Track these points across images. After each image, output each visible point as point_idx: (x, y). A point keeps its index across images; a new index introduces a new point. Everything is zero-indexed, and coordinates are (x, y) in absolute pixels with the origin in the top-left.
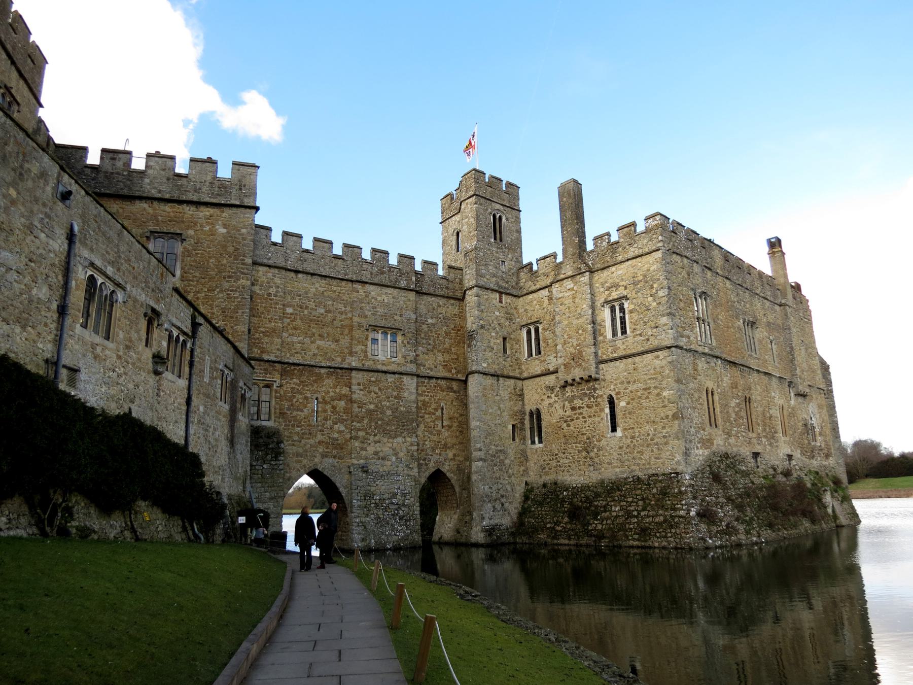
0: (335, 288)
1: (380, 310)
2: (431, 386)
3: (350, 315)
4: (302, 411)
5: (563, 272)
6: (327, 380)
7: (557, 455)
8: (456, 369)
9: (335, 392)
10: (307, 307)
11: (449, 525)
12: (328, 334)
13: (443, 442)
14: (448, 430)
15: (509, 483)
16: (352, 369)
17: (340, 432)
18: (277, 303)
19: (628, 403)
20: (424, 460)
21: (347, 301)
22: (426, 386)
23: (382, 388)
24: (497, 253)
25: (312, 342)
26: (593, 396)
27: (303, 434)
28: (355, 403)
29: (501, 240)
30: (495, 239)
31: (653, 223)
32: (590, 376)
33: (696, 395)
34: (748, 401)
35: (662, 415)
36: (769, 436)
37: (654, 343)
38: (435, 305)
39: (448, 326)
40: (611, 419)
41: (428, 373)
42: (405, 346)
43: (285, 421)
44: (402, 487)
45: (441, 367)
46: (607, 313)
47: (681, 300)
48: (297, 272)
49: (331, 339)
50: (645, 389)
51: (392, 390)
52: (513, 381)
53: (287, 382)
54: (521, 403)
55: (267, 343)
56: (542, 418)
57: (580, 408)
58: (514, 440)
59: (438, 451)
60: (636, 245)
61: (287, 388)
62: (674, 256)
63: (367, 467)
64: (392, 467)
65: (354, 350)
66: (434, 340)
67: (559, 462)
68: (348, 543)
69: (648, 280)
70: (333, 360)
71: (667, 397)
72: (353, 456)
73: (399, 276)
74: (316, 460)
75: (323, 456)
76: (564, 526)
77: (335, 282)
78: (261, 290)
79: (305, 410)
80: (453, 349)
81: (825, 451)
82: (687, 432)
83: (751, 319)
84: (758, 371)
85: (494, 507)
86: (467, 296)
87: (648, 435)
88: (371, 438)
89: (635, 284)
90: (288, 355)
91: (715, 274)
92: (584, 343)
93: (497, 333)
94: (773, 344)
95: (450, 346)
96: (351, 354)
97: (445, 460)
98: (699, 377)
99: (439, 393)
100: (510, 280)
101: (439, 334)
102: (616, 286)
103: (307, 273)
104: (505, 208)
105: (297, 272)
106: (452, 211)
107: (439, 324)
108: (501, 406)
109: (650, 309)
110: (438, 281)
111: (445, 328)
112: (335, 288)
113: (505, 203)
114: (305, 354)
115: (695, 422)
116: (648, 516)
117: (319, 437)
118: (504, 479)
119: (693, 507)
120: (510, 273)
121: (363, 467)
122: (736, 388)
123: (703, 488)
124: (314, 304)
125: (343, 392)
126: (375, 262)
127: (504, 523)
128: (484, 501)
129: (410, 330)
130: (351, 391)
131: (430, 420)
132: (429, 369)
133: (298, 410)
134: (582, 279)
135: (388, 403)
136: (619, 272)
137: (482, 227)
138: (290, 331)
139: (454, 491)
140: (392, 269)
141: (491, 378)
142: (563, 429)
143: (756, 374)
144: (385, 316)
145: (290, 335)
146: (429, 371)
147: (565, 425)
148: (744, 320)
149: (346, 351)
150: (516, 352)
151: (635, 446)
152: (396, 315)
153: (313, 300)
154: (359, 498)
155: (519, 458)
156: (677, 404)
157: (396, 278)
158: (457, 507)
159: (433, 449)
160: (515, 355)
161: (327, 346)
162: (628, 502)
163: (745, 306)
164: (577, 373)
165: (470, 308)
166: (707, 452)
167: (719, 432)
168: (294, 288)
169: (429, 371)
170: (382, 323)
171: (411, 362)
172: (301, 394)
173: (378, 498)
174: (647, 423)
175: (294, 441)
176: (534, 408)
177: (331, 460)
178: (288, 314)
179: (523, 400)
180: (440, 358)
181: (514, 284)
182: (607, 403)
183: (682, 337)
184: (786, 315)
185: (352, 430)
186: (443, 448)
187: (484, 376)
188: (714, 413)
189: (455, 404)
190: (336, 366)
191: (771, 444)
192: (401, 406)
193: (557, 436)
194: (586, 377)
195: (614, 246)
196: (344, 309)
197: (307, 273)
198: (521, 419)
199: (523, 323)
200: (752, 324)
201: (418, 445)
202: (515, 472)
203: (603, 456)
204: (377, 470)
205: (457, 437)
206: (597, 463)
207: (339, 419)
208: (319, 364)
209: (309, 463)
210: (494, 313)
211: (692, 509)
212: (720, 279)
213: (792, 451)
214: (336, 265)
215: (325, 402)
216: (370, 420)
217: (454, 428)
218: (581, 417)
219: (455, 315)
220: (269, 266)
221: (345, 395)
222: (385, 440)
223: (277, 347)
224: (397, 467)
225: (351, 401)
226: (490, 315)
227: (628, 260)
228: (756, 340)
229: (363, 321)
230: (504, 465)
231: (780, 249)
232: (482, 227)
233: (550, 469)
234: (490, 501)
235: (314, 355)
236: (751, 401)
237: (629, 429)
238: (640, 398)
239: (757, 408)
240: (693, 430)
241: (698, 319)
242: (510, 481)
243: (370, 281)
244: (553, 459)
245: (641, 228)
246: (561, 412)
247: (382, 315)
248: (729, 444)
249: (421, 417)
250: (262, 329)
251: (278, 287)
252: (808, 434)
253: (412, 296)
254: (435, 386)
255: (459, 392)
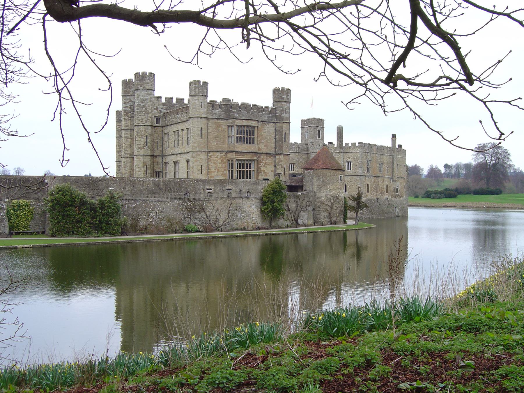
34: (378, 185)
46: (347, 164)
69: (357, 159)
102: (350, 158)
136: (351, 154)
143: (381, 178)
166: (366, 199)
191: (382, 195)
195: (350, 147)
239: (380, 187)
245: (357, 145)
253: (297, 154)
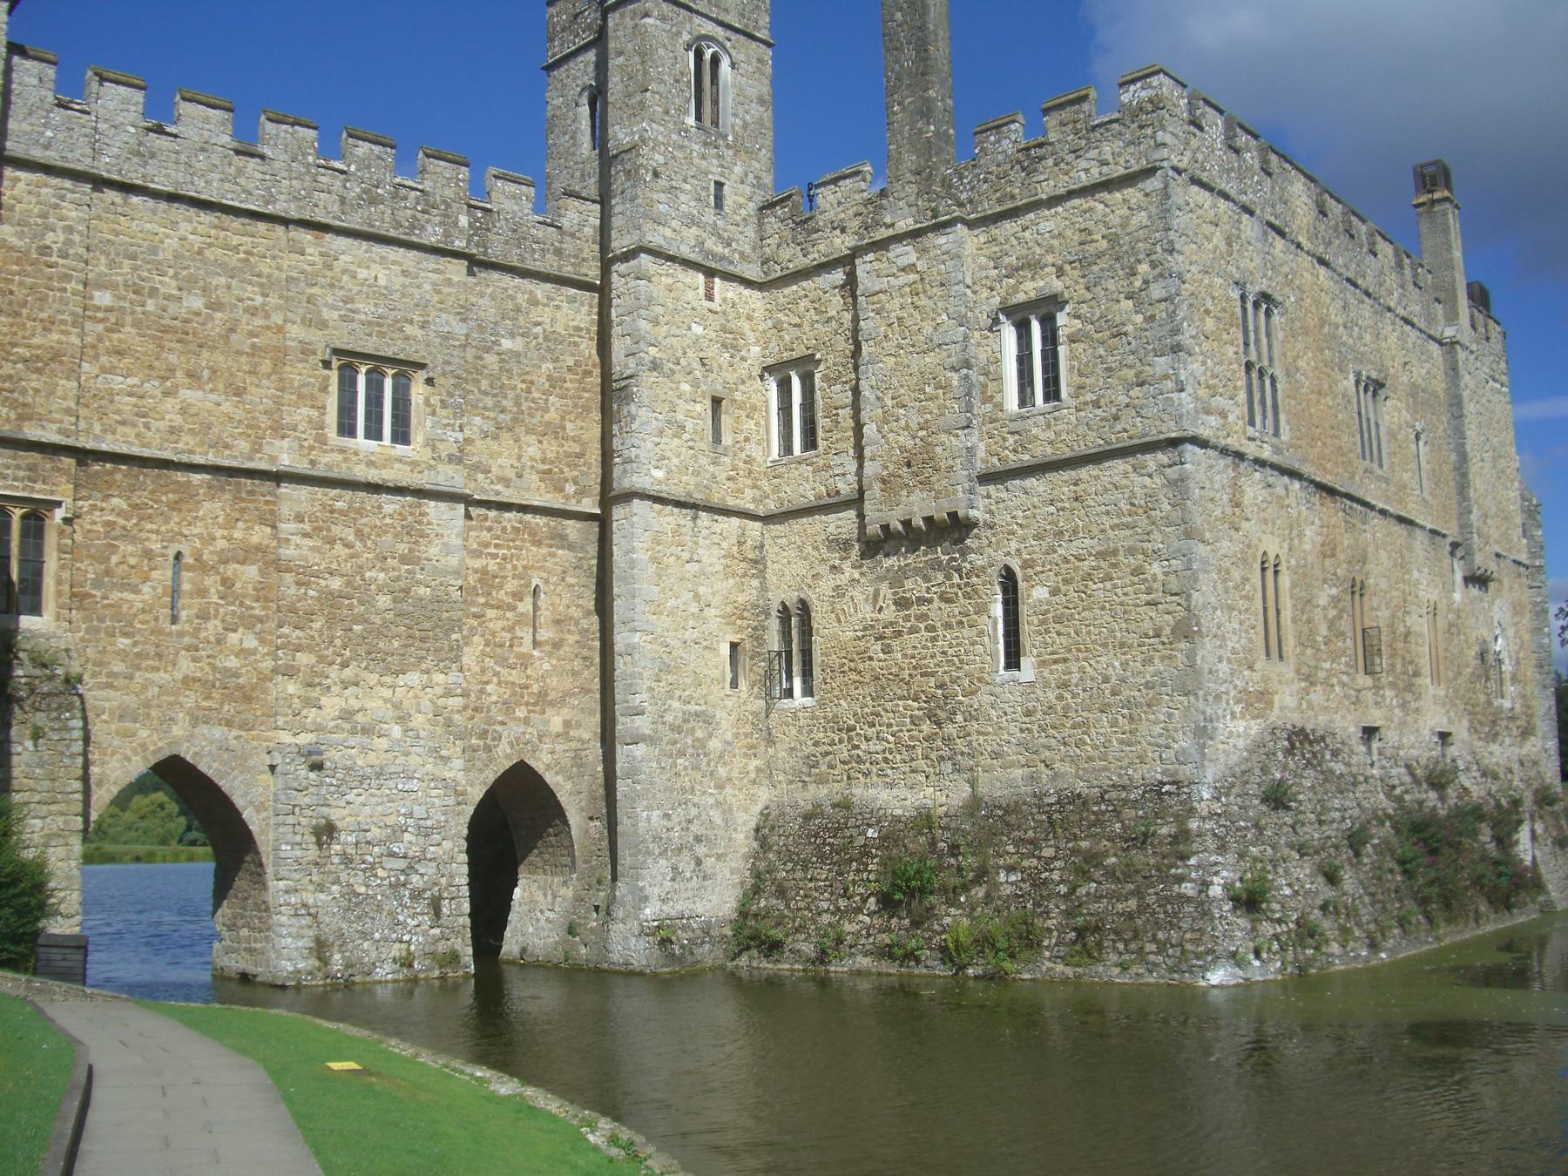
0: (235, 240)
1: (366, 309)
2: (504, 529)
3: (277, 319)
4: (137, 591)
5: (888, 220)
6: (207, 505)
7: (853, 729)
8: (576, 483)
9: (229, 539)
10: (153, 292)
11: (548, 914)
12: (215, 372)
13: (535, 688)
14: (550, 655)
15: (718, 804)
16: (279, 477)
17: (243, 653)
18: (68, 278)
19: (1054, 592)
20: (484, 734)
21: (269, 276)
22: (490, 529)
23: (367, 530)
24: (703, 157)
25: (167, 394)
26: (958, 570)
27: (138, 655)
28: (289, 570)
29: (715, 123)
30: (699, 118)
31: (1144, 94)
32: (953, 515)
33: (1236, 574)
34: (1357, 589)
35: (1147, 626)
36: (1401, 685)
37: (1134, 428)
38: (521, 299)
39: (556, 360)
40: (1007, 635)
41: (498, 493)
42: (434, 413)
43: (87, 619)
44: (419, 811)
45: (535, 477)
47: (1207, 312)
48: (127, 188)
49: (221, 386)
50: (1101, 555)
51: (396, 536)
52: (735, 521)
53: (94, 507)
54: (755, 583)
55: (37, 391)
56: (815, 626)
57: (922, 601)
58: (734, 684)
59: (521, 712)
60: (1093, 153)
61: (95, 523)
62: (1195, 189)
63: (320, 753)
64: (390, 755)
65: (287, 420)
66: (518, 397)
67: (856, 747)
68: (268, 960)
70: (226, 446)
71: (1161, 577)
72: (280, 723)
73: (423, 212)
74: (177, 731)
75: (195, 721)
76: (867, 919)
77: (236, 223)
78: (20, 235)
79: (146, 589)
80: (569, 426)
81: (1522, 722)
82: (1210, 672)
83: (1374, 375)
84: (1383, 512)
85: (674, 868)
86: (615, 278)
87: (1106, 680)
88: (334, 672)
89: (1084, 262)
90: (97, 428)
91: (1293, 247)
92: (941, 421)
93: (695, 384)
94: (1421, 443)
95: (563, 418)
96: (279, 430)
97: (540, 737)
98: (1245, 525)
99: (528, 550)
100: (737, 236)
101: (532, 383)
102: (1033, 266)
103: (157, 195)
104: (729, 33)
105: (127, 188)
106: (577, 35)
107: (532, 354)
108: (701, 590)
109: (1125, 334)
110: (534, 232)
111: (547, 366)
112: (235, 240)
113: (728, 19)
114: (147, 426)
115: (1230, 645)
116: (1098, 898)
117: (186, 666)
118: (704, 793)
119: (1216, 873)
120: (737, 218)
121: (310, 753)
122: (1333, 556)
123: (1242, 823)
124: (174, 283)
125: (255, 539)
126: (353, 168)
127: (700, 910)
128: (649, 853)
129: (448, 368)
130: (275, 537)
131: (500, 624)
132: (501, 479)
133: (124, 587)
134: (942, 240)
135: (382, 575)
136: (1048, 222)
137: (662, 81)
138: (104, 359)
139: (566, 822)
140: (403, 191)
141: (676, 510)
142: (871, 659)
143: (1377, 521)
144: (379, 325)
145: (104, 370)
146: (499, 487)
147: (878, 648)
148: (1358, 375)
149: (264, 422)
150: (747, 440)
151: (1066, 709)
152: (411, 322)
153: (171, 272)
154: (298, 838)
155: (746, 735)
156: (1189, 597)
157: (414, 217)
158: (573, 866)
159: (508, 707)
160: (742, 449)
161: (209, 405)
162: (1039, 858)
163: (1360, 338)
164: (918, 506)
165: (620, 310)
166: (1255, 727)
167: (1287, 669)
168: (117, 234)
169: (499, 487)
170: (369, 348)
171: (451, 459)
172: (134, 540)
173: (352, 839)
174: (1105, 645)
175: (111, 674)
176: (791, 598)
177: (218, 732)
178: (98, 309)
179: (761, 575)
180: (533, 450)
181: (747, 249)
182: (998, 589)
183: (1208, 412)
184: (1455, 369)
185: (278, 648)
186: (535, 704)
187: (657, 507)
188: (1278, 622)
189: (572, 580)
190: (235, 464)
192: (419, 583)
193: (854, 676)
194: (941, 515)
196: (259, 299)
197: (157, 195)
198: (755, 629)
199: (770, 361)
200: (1376, 387)
201: (465, 694)
202: (735, 774)
203: (979, 733)
204: (349, 763)
205: (575, 674)
206: (962, 754)
207: (240, 617)
208: (185, 458)
209: (155, 737)
210: (689, 328)
211: (1215, 879)
212: (1306, 261)
213: (1450, 721)
214: (240, 172)
215: (201, 566)
216: (331, 621)
217: (566, 650)
218: (922, 626)
219: (578, 329)
220: (48, 169)
221: (260, 549)
222: (373, 678)
223: (65, 404)
224: (407, 754)
225: (278, 565)
226: (678, 332)
227: (1071, 194)
228: (1383, 430)
229: (316, 337)
230: (706, 755)
231: (1446, 193)
232: (662, 81)
233: (831, 767)
234: (663, 854)
235: (173, 431)
236: (1367, 593)
237: (1056, 662)
238: (1089, 577)
240: (1223, 668)
241: (1249, 366)
242: (720, 798)
243: (337, 223)
244: (841, 741)
246: (867, 612)
247: (370, 323)
248: (1310, 706)
249: (476, 616)
250: (20, 350)
251: (70, 230)
252: (1488, 679)
253: (457, 269)
254: (517, 530)
255: (582, 548)
